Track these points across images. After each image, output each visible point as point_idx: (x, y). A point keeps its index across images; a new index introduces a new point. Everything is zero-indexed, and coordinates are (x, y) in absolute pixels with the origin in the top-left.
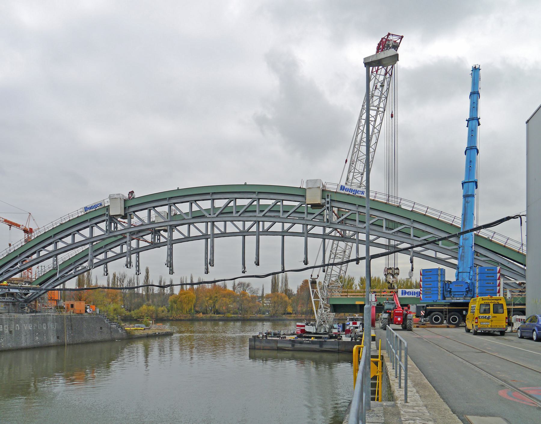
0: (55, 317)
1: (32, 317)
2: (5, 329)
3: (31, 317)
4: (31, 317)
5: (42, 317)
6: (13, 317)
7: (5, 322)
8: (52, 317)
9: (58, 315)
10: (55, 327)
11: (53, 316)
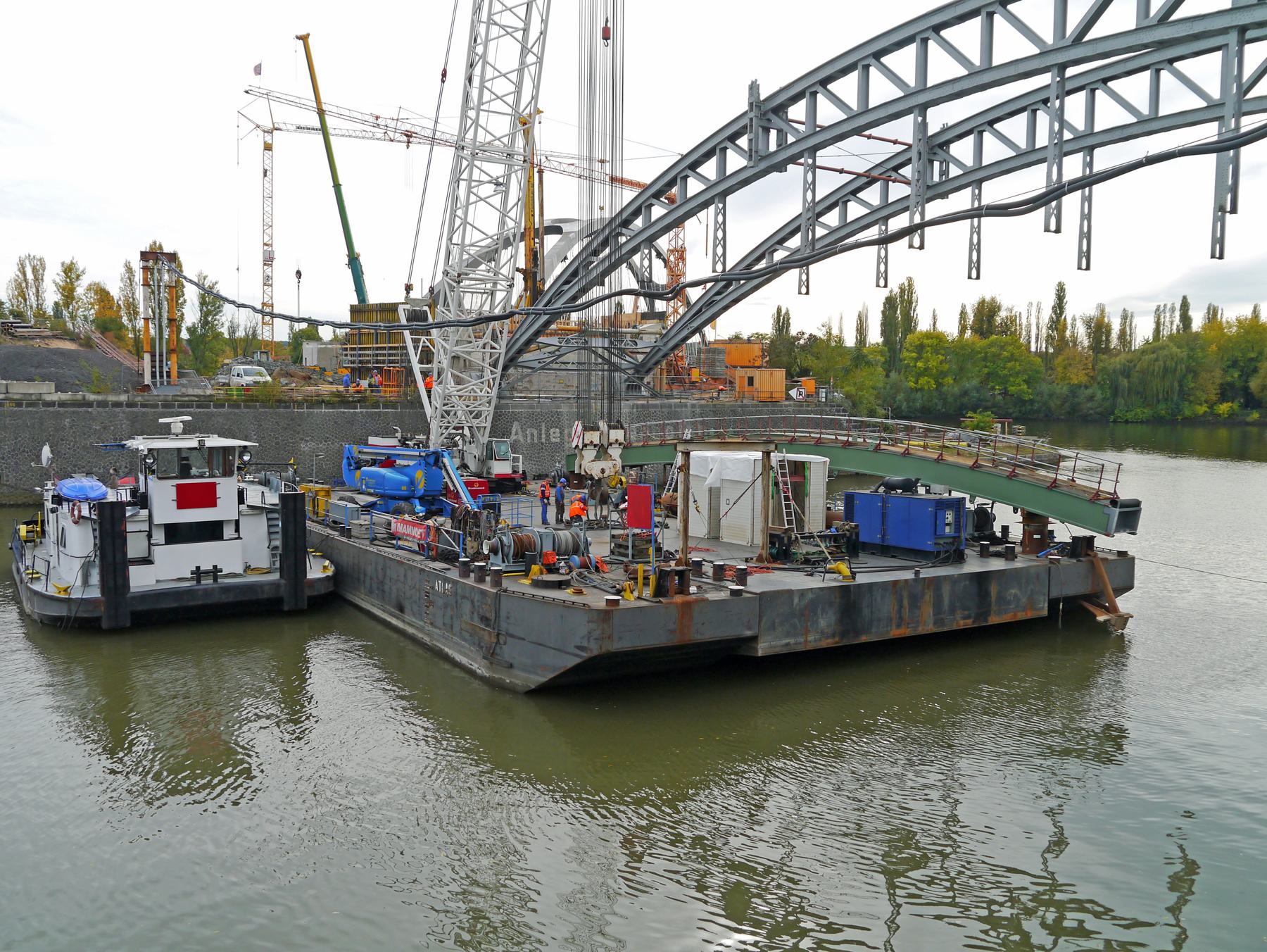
0: (698, 410)
1: (637, 408)
3: (635, 410)
4: (635, 410)
5: (663, 410)
8: (689, 409)
11: (693, 406)
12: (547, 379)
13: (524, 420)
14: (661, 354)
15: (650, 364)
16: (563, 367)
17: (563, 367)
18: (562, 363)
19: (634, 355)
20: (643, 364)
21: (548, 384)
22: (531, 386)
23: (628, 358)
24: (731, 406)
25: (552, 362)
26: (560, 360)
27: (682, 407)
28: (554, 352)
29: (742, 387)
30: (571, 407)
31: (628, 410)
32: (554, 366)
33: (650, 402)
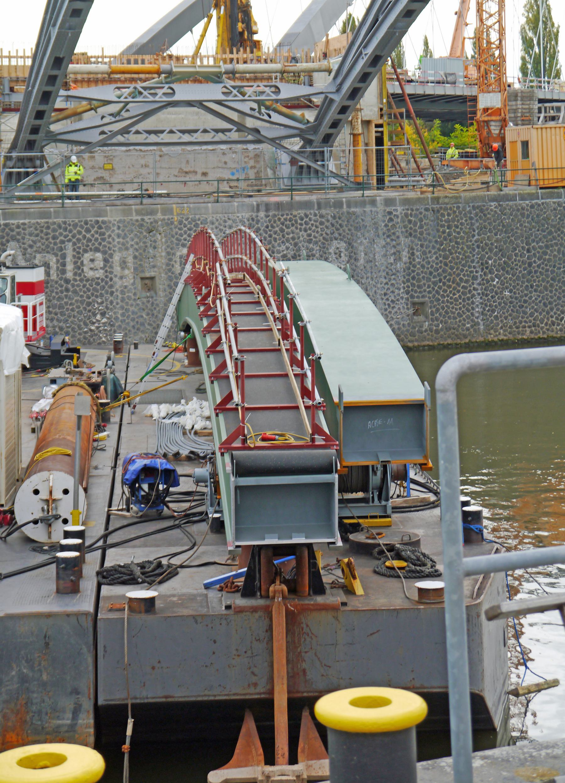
0: (400, 210)
1: (267, 210)
2: (117, 269)
4: (262, 214)
5: (323, 212)
6: (159, 216)
7: (119, 236)
8: (380, 207)
9: (419, 200)
10: (397, 256)
11: (389, 202)
12: (143, 162)
13: (28, 240)
14: (335, 108)
15: (324, 129)
16: (153, 138)
17: (153, 138)
18: (149, 132)
19: (298, 113)
20: (315, 128)
21: (144, 171)
22: (111, 176)
23: (276, 118)
24: (474, 199)
25: (125, 131)
26: (140, 127)
27: (363, 204)
28: (119, 113)
29: (514, 162)
30: (127, 212)
31: (247, 215)
32: (132, 138)
33: (297, 198)
